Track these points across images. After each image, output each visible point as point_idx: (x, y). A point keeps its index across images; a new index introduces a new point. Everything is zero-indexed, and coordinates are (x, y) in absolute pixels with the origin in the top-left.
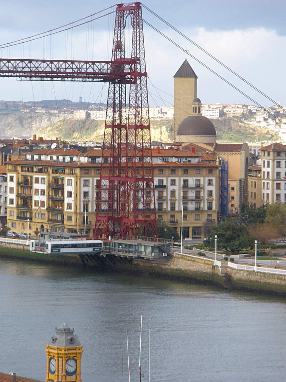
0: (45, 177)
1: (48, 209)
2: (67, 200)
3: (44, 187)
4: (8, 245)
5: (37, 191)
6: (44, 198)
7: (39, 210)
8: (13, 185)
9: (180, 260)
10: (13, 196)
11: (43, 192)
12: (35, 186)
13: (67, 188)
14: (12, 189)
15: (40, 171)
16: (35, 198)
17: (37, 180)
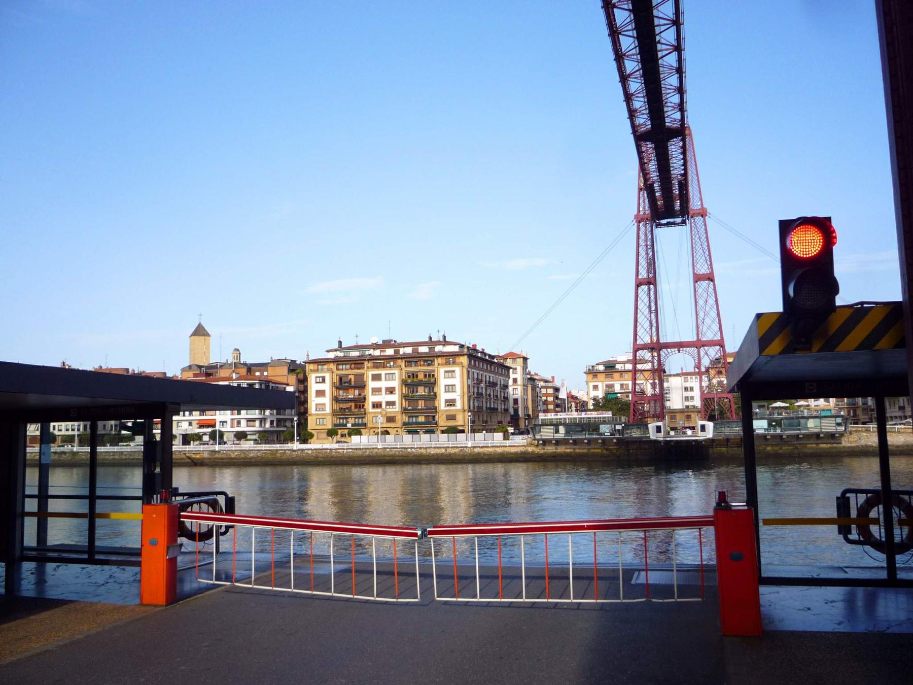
0: (396, 372)
1: (404, 411)
2: (443, 396)
3: (395, 384)
4: (423, 451)
5: (377, 391)
6: (395, 398)
7: (384, 413)
8: (327, 387)
9: (865, 434)
10: (327, 400)
11: (391, 391)
12: (371, 384)
13: (443, 381)
14: (320, 393)
15: (376, 367)
16: (372, 399)
17: (377, 378)
